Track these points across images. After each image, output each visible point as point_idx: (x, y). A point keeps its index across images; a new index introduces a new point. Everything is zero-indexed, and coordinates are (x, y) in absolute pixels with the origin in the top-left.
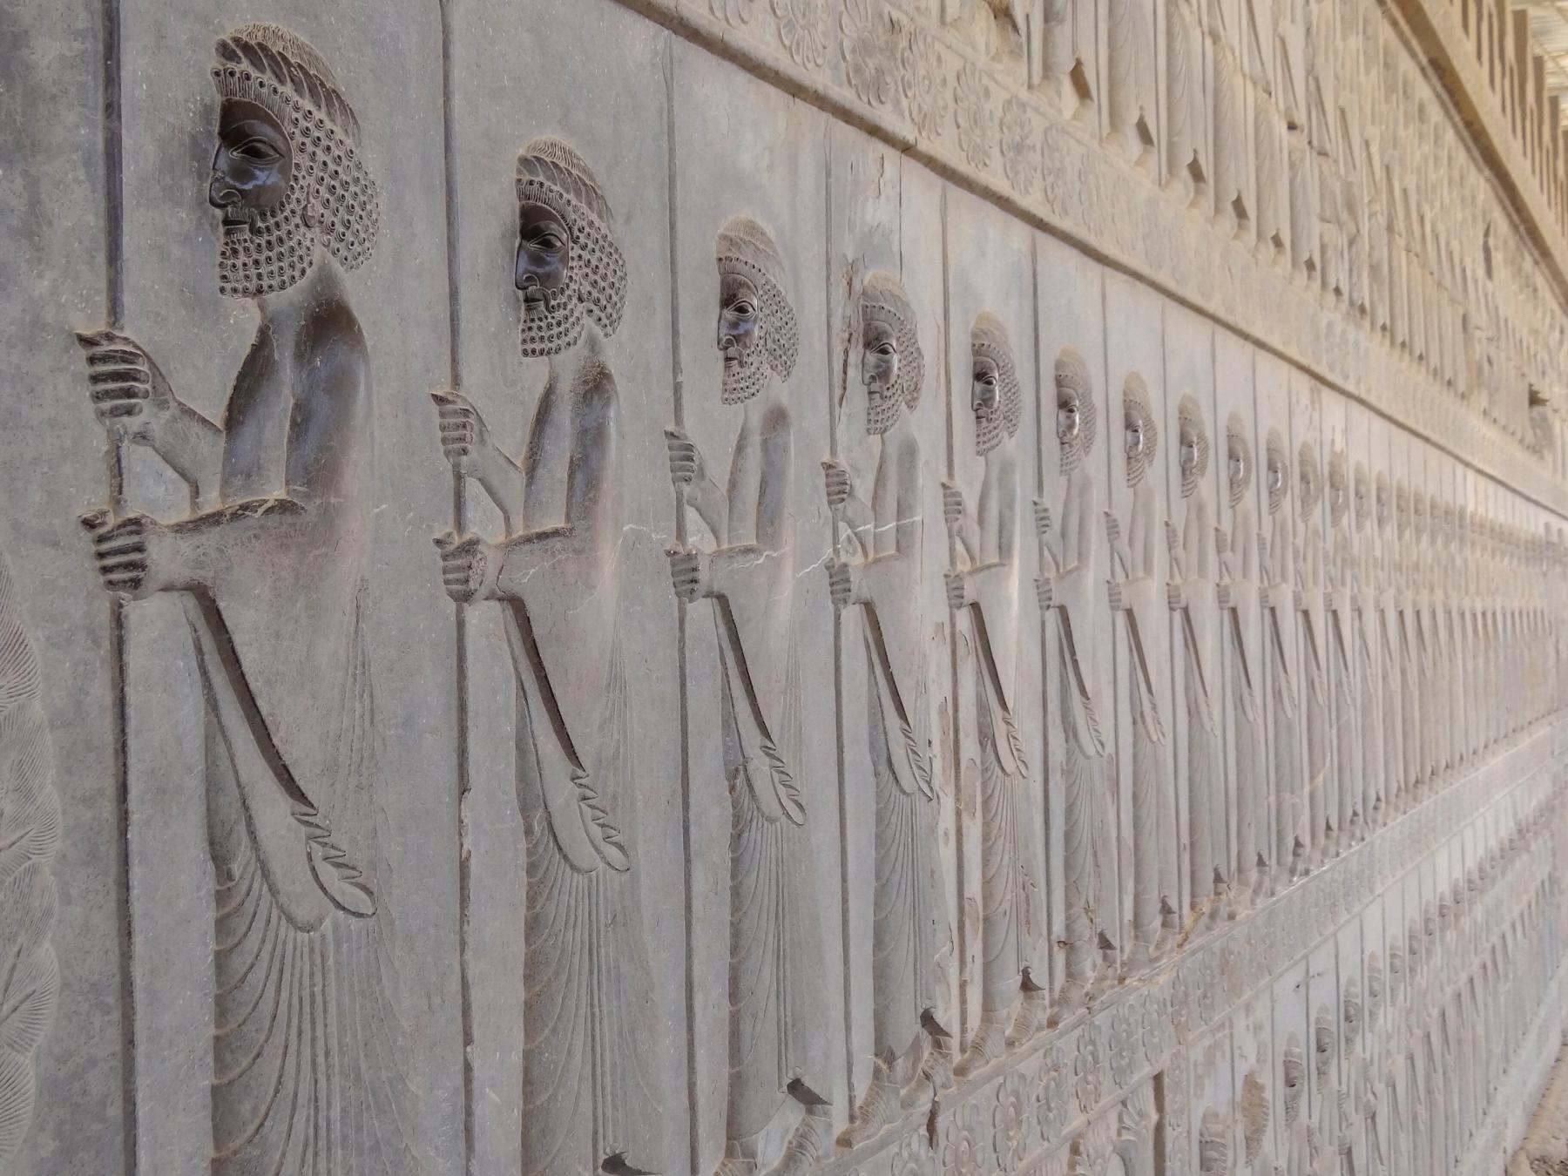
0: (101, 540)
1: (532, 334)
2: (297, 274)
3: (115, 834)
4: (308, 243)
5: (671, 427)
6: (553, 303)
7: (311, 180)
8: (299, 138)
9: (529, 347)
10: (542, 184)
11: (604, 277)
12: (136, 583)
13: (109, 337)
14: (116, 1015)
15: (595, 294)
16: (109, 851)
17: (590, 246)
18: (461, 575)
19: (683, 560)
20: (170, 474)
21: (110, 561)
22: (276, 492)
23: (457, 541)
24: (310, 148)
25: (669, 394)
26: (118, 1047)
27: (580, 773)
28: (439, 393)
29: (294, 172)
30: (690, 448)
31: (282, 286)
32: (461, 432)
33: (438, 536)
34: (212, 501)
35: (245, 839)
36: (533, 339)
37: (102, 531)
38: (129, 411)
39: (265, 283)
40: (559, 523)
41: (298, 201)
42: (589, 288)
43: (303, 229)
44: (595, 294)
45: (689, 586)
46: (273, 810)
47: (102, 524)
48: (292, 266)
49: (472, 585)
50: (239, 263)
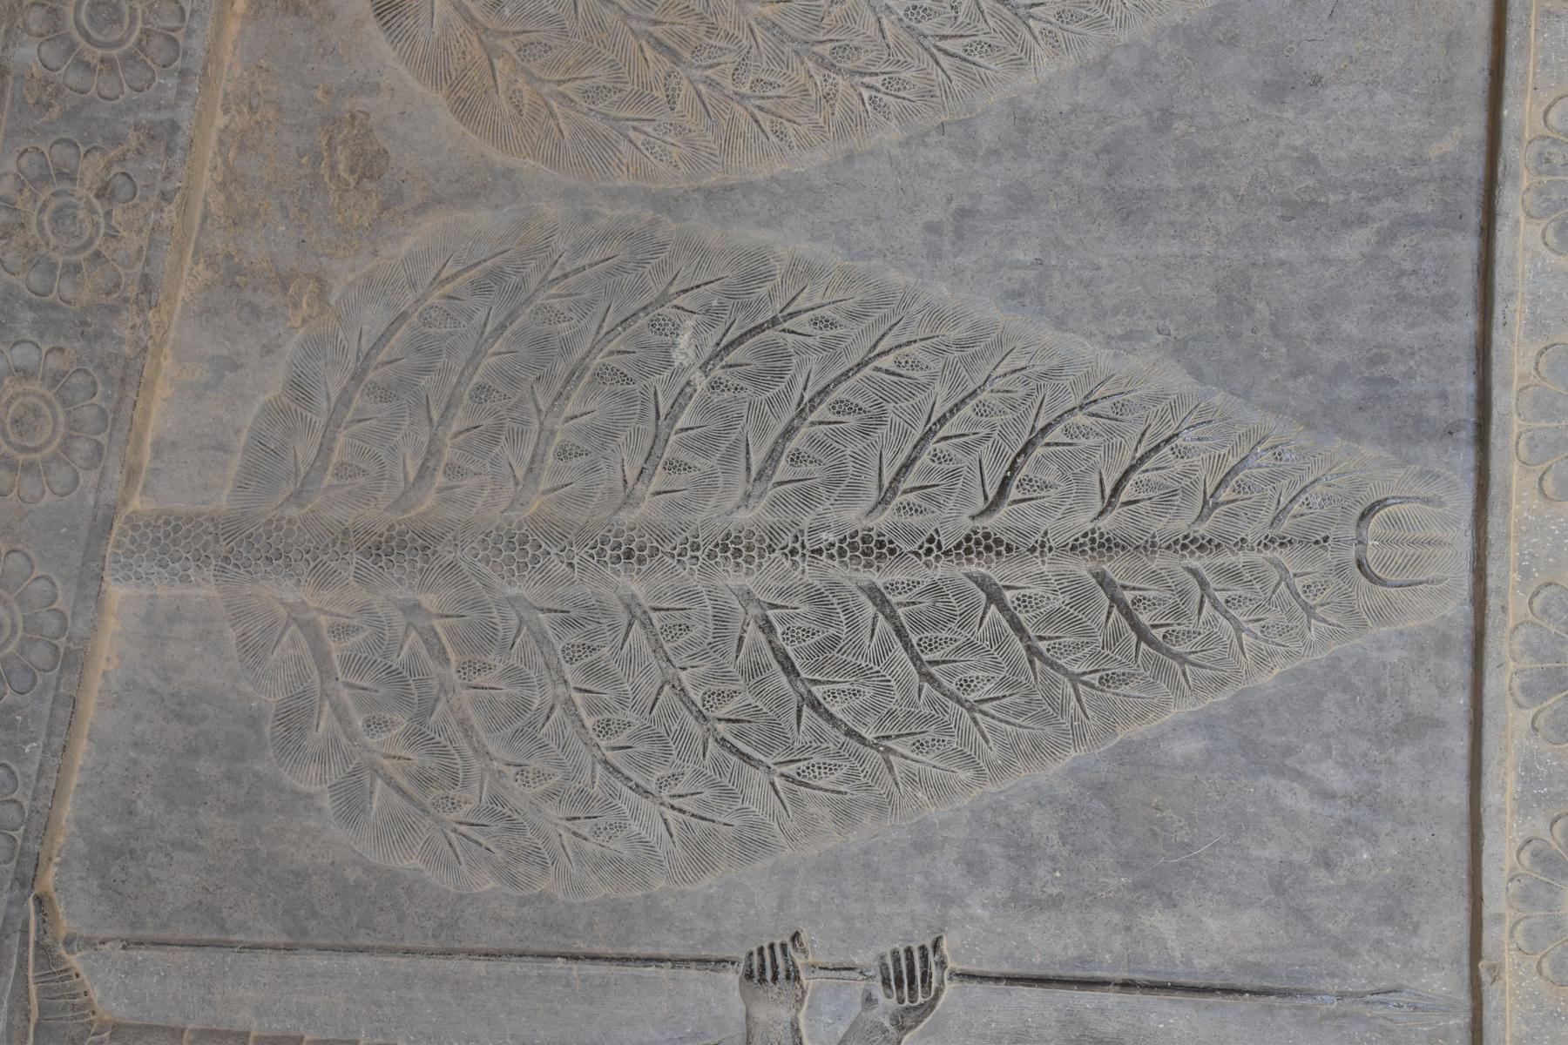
0: (783, 946)
3: (563, 950)
14: (431, 944)
16: (553, 943)
26: (408, 944)
37: (790, 947)
47: (794, 946)
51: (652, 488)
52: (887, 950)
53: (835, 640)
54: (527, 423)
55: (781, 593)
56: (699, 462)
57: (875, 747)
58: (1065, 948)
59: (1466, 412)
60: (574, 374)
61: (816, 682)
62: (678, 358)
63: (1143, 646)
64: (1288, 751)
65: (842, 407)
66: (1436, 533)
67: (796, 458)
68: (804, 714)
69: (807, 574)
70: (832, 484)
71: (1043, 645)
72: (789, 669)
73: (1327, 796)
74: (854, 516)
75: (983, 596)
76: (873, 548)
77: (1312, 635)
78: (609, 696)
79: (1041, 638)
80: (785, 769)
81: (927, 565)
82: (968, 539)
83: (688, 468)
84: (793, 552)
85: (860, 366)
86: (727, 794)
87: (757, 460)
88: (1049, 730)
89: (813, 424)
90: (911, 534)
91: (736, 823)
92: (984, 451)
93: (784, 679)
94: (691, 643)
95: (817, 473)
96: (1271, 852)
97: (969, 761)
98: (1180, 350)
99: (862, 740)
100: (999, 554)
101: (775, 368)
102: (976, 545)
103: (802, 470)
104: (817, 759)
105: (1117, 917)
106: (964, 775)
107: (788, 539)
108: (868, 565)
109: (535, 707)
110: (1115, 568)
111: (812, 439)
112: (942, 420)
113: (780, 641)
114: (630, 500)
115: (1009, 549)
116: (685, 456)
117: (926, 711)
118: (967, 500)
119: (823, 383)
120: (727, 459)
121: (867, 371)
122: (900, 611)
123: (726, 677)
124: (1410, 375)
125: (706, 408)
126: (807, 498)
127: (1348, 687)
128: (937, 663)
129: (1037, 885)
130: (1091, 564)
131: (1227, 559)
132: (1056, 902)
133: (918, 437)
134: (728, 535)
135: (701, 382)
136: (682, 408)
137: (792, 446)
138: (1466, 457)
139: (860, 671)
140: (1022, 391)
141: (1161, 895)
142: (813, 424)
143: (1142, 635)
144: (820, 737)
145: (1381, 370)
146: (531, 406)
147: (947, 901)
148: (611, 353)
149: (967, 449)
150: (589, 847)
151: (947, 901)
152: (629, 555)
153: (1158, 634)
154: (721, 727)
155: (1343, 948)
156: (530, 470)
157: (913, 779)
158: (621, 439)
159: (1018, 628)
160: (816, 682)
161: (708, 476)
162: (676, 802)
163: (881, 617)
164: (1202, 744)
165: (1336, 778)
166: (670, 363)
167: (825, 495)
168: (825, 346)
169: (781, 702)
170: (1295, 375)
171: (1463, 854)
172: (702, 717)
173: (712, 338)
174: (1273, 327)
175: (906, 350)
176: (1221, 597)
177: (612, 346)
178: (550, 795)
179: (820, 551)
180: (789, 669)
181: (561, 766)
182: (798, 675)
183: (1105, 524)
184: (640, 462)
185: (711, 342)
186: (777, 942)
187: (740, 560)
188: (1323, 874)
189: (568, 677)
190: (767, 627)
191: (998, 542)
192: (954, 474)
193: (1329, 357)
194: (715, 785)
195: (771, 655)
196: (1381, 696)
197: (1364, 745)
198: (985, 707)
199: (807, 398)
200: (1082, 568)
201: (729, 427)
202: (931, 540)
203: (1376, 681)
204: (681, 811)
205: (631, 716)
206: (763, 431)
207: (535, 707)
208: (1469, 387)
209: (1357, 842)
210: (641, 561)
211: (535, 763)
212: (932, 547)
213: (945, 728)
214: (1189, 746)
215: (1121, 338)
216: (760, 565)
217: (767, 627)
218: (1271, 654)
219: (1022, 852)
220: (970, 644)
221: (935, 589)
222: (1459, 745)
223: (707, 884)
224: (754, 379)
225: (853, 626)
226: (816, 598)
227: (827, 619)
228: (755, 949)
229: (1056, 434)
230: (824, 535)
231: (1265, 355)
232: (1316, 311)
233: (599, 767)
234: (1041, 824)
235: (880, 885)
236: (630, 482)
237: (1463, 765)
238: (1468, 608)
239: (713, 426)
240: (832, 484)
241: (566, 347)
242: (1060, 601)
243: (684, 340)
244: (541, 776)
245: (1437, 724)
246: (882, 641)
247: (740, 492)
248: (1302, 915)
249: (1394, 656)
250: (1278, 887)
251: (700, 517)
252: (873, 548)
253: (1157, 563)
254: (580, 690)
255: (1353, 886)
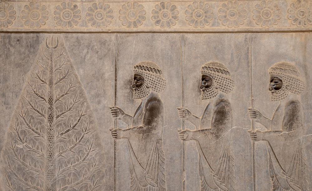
0: (112, 132)
1: (204, 96)
2: (146, 95)
4: (148, 90)
5: (251, 108)
6: (207, 90)
7: (149, 82)
8: (145, 77)
9: (203, 98)
10: (205, 71)
11: (223, 84)
12: (116, 138)
13: (113, 107)
15: (221, 87)
16: (112, 170)
17: (218, 79)
18: (182, 136)
19: (252, 134)
20: (125, 123)
21: (113, 135)
22: (141, 125)
23: (182, 131)
24: (147, 77)
25: (251, 102)
27: (213, 171)
28: (179, 108)
29: (145, 81)
30: (255, 112)
31: (144, 97)
32: (182, 114)
33: (179, 130)
34: (131, 127)
35: (134, 172)
36: (203, 97)
38: (117, 116)
39: (141, 97)
40: (210, 128)
41: (145, 85)
42: (219, 86)
43: (147, 89)
44: (221, 87)
45: (254, 138)
46: (138, 169)
48: (145, 94)
49: (184, 138)
50: (136, 95)
51: (41, 152)
52: (112, 116)
53: (64, 123)
54: (30, 172)
55: (57, 132)
56: (37, 144)
57: (80, 117)
58: (111, 89)
59: (35, 35)
60: (23, 164)
61: (70, 126)
62: (22, 147)
63: (66, 78)
64: (81, 57)
65: (30, 122)
66: (51, 38)
67: (37, 129)
68: (75, 128)
69: (54, 128)
70: (41, 123)
71: (65, 92)
72: (68, 131)
73: (88, 52)
74: (46, 120)
75: (58, 101)
76: (51, 118)
77: (65, 54)
78: (73, 160)
79: (64, 92)
80: (84, 131)
81: (53, 109)
82: (49, 103)
83: (38, 146)
84: (50, 130)
85: (24, 119)
86: (88, 141)
87: (37, 135)
88: (78, 91)
89: (32, 126)
90: (48, 111)
91: (93, 139)
92: (37, 100)
93: (70, 131)
94: (64, 146)
95: (39, 126)
96: (96, 60)
97: (83, 103)
98: (25, 73)
99: (79, 119)
100: (52, 98)
101: (24, 132)
102: (50, 101)
103: (39, 129)
104: (82, 126)
105: (106, 81)
106: (85, 104)
107: (49, 130)
108: (53, 118)
109: (74, 172)
110: (54, 82)
111: (34, 127)
112: (32, 107)
113: (64, 132)
114: (43, 155)
115: (51, 97)
116: (36, 147)
117: (75, 110)
118: (44, 103)
119: (26, 125)
120: (37, 140)
121: (25, 118)
122: (60, 113)
123: (70, 141)
124: (30, 42)
125: (29, 143)
126: (43, 127)
127: (72, 49)
128: (68, 108)
129: (102, 93)
130: (54, 85)
131: (53, 66)
132: (104, 90)
133: (34, 110)
134: (48, 140)
135: (25, 144)
136: (29, 147)
137: (35, 130)
138: (41, 34)
139: (69, 119)
140: (29, 95)
141: (103, 75)
142: (32, 126)
143: (64, 78)
144: (79, 126)
145: (29, 46)
146: (28, 171)
147: (105, 107)
148: (20, 158)
149: (36, 103)
150: (97, 164)
151: (105, 107)
152: (50, 156)
153: (64, 75)
154: (77, 141)
155: (109, 50)
156: (37, 172)
157: (86, 112)
158: (33, 157)
159: (63, 96)
160: (70, 126)
161: (39, 143)
162: (89, 149)
163: (61, 116)
164: (81, 69)
165: (85, 51)
166: (22, 149)
167: (42, 125)
168: (21, 124)
169: (73, 132)
170: (29, 57)
171: (95, 34)
172: (76, 145)
173: (19, 142)
174: (23, 60)
175: (22, 112)
176: (59, 67)
177: (19, 158)
178: (89, 170)
179: (50, 126)
180: (68, 131)
181: (84, 168)
182: (69, 129)
183: (48, 83)
184: (37, 154)
185: (20, 142)
186: (111, 133)
187: (52, 138)
188: (99, 53)
189: (69, 166)
190: (62, 134)
191: (50, 99)
192: (40, 105)
193: (27, 52)
194: (87, 142)
195: (66, 134)
196: (74, 45)
197: (81, 47)
198: (74, 101)
199: (28, 127)
200: (54, 86)
201: (32, 139)
202: (49, 108)
203: (72, 46)
204: (91, 148)
205: (76, 156)
206: (33, 134)
207: (74, 172)
208: (32, 34)
209: (94, 48)
210: (51, 154)
211: (84, 172)
212: (51, 108)
213: (78, 107)
214: (81, 71)
215: (23, 81)
216: (53, 135)
217: (62, 134)
218: (68, 60)
219: (98, 95)
220: (65, 103)
221: (57, 108)
222: (80, 35)
223: (103, 144)
224: (25, 135)
225: (62, 120)
226: (58, 126)
227: (61, 124)
228: (113, 137)
229: (35, 90)
230: (48, 125)
231: (26, 61)
232: (21, 54)
233: (84, 162)
234: (93, 93)
235: (102, 117)
236: (40, 155)
237: (83, 34)
238: (62, 34)
239: (32, 142)
240: (41, 123)
241: (19, 165)
242: (59, 89)
243: (19, 146)
244: (86, 171)
245: (77, 38)
246: (64, 116)
247: (42, 138)
248: (105, 56)
249: (68, 44)
250: (101, 59)
251: (45, 144)
252: (51, 118)
253: (54, 76)
254: (72, 164)
255: (100, 49)
